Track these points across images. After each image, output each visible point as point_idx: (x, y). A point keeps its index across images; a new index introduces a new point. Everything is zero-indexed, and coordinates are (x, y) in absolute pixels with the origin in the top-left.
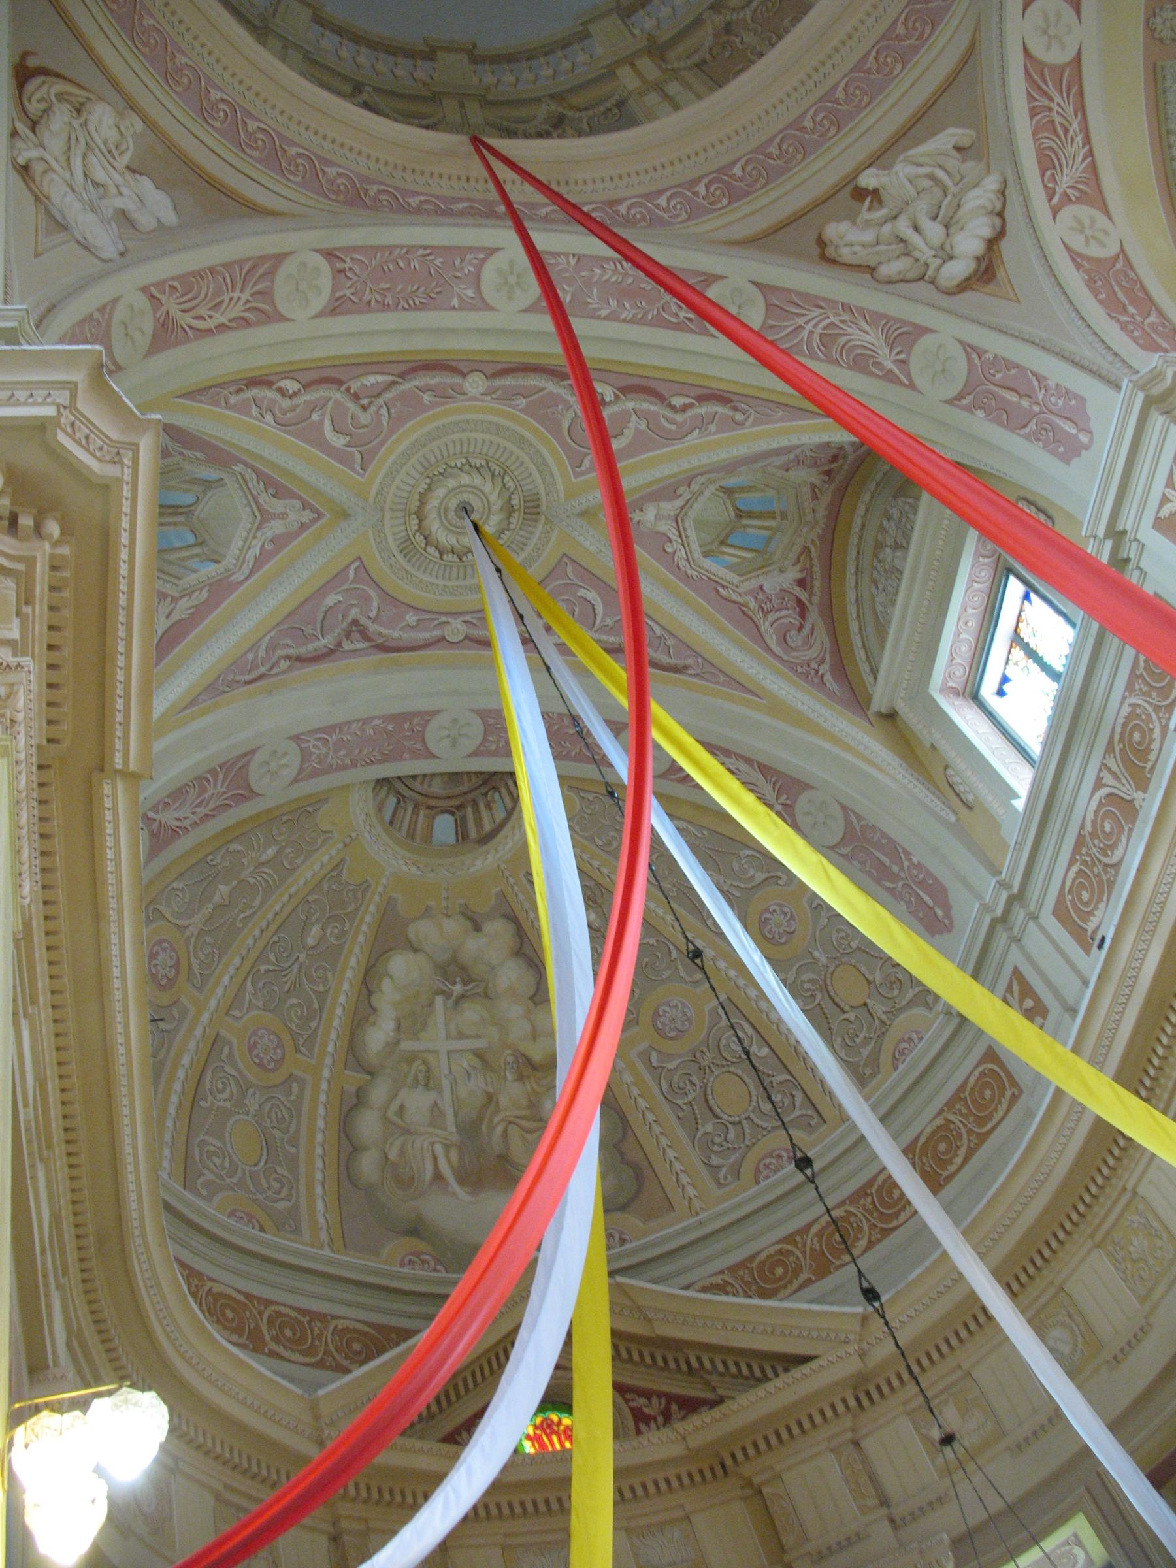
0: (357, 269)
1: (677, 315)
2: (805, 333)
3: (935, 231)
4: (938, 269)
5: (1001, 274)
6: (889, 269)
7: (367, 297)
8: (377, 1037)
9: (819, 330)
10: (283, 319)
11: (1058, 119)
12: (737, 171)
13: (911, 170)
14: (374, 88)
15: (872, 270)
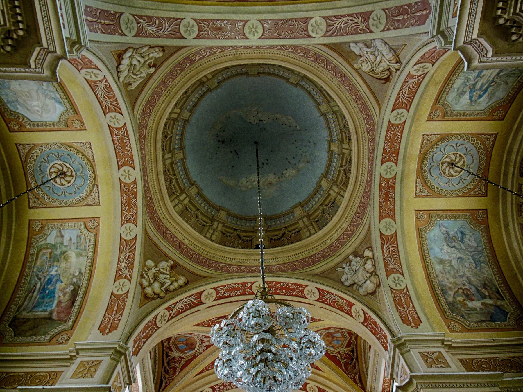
0: (300, 32)
1: (204, 24)
2: (167, 25)
3: (135, 62)
4: (133, 53)
5: (116, 57)
6: (145, 49)
7: (297, 23)
9: (164, 27)
10: (324, 18)
11: (108, 100)
12: (188, 64)
13: (142, 75)
15: (150, 47)
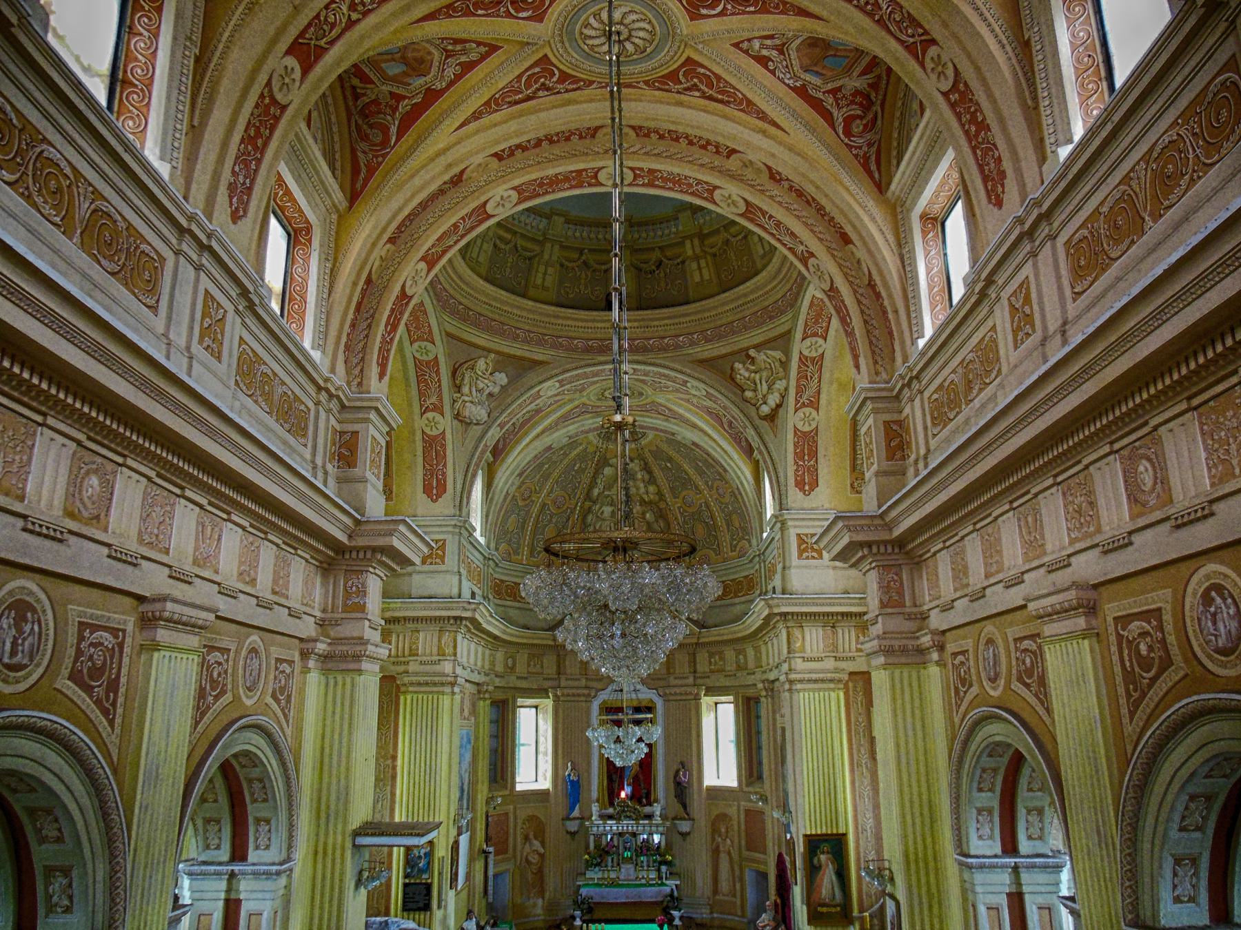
6: (749, 394)
8: (596, 492)
14: (590, 250)
